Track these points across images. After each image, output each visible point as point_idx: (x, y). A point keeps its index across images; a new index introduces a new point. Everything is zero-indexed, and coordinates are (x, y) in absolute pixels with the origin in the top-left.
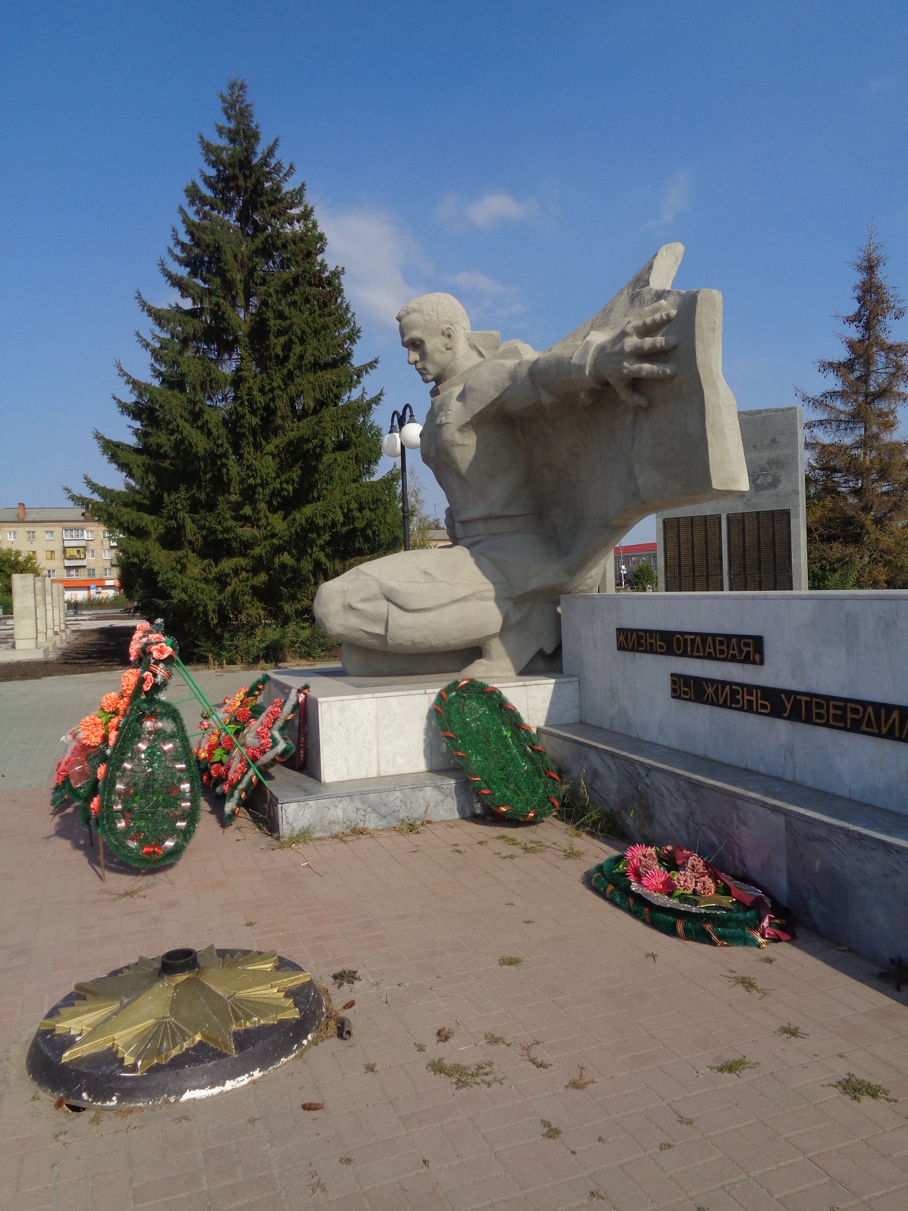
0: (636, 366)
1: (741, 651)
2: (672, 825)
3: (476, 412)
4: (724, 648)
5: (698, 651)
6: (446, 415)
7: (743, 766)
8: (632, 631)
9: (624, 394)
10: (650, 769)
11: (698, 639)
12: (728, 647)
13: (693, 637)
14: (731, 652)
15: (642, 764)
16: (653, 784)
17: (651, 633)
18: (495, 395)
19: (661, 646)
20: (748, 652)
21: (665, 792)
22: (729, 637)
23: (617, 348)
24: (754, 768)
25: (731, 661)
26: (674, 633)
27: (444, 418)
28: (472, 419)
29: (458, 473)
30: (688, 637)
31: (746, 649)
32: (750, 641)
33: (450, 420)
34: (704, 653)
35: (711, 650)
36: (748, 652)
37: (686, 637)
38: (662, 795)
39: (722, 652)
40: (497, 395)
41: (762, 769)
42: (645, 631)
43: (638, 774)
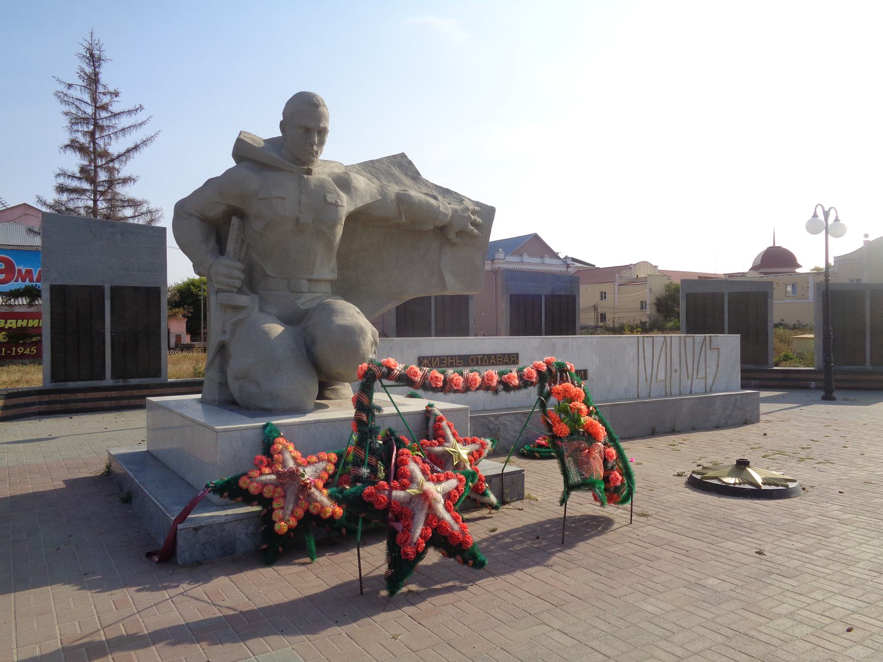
0: (472, 228)
1: (510, 360)
2: (512, 436)
3: (359, 206)
4: (501, 359)
5: (486, 362)
6: (340, 199)
7: (506, 407)
8: (435, 357)
9: (452, 236)
10: (497, 417)
11: (485, 357)
12: (503, 359)
13: (482, 356)
14: (505, 361)
15: (493, 416)
16: (500, 422)
17: (452, 357)
18: (368, 200)
19: (459, 363)
20: (514, 360)
21: (508, 423)
22: (504, 355)
23: (466, 215)
24: (512, 406)
25: (505, 365)
26: (470, 356)
27: (339, 202)
28: (355, 210)
29: (329, 245)
30: (479, 357)
31: (512, 359)
32: (515, 355)
33: (344, 205)
34: (489, 362)
35: (494, 361)
36: (514, 360)
37: (477, 357)
38: (506, 425)
39: (500, 361)
40: (371, 202)
41: (516, 406)
42: (447, 357)
43: (490, 421)
